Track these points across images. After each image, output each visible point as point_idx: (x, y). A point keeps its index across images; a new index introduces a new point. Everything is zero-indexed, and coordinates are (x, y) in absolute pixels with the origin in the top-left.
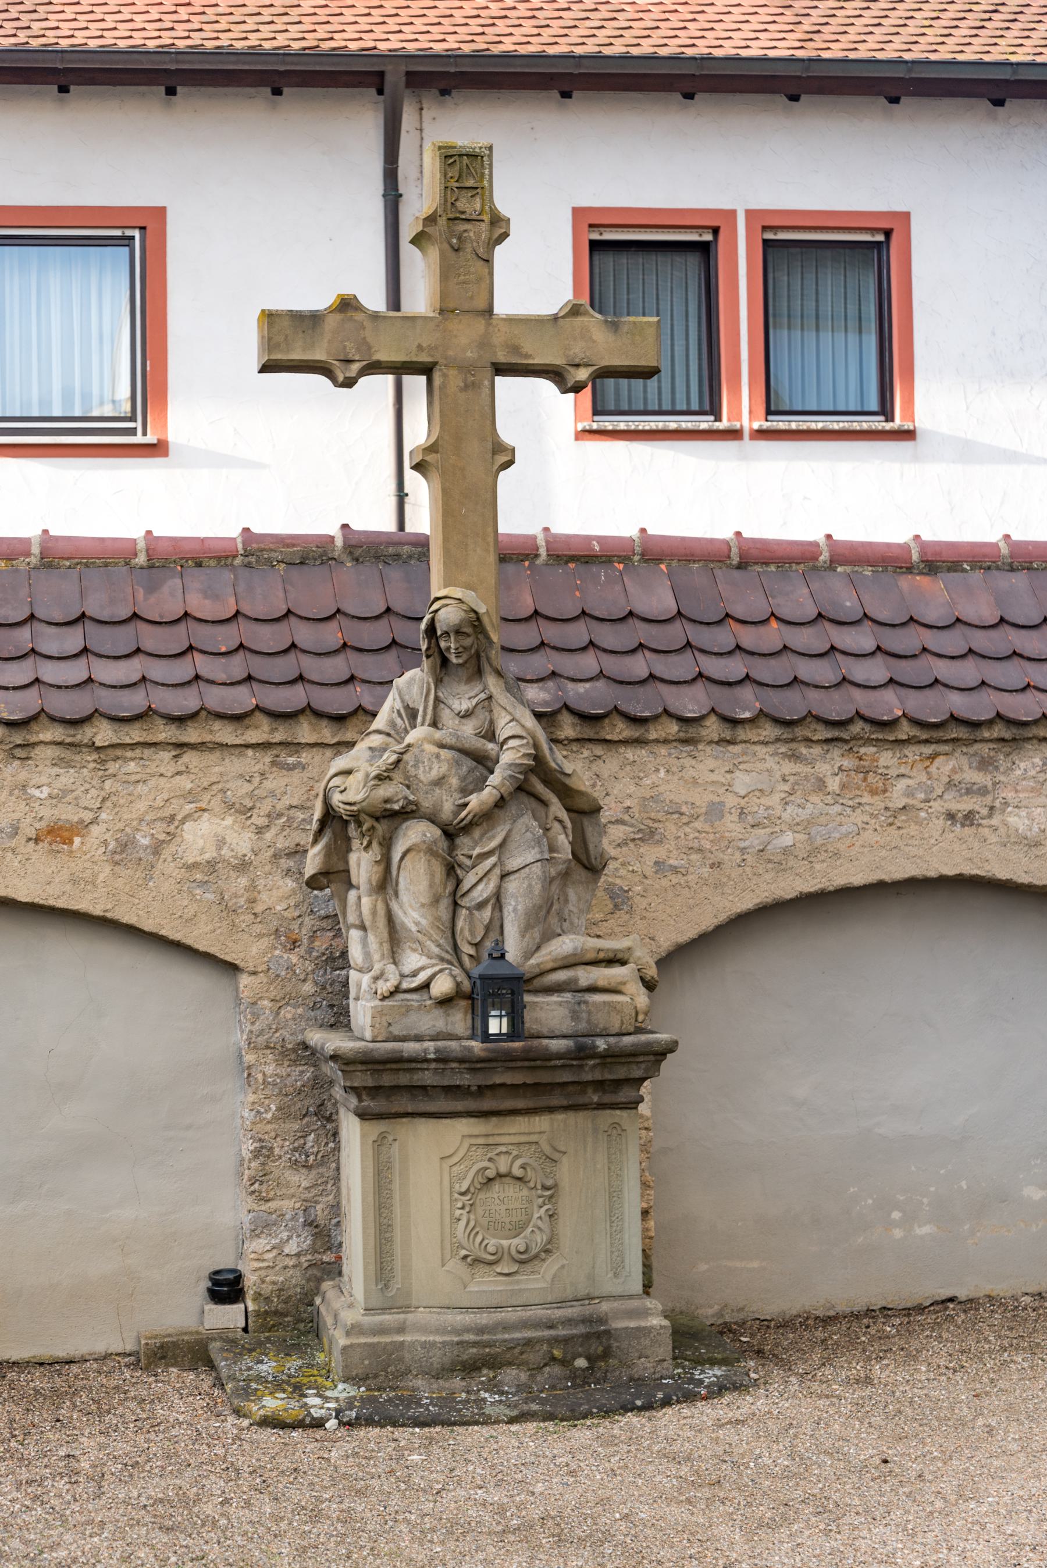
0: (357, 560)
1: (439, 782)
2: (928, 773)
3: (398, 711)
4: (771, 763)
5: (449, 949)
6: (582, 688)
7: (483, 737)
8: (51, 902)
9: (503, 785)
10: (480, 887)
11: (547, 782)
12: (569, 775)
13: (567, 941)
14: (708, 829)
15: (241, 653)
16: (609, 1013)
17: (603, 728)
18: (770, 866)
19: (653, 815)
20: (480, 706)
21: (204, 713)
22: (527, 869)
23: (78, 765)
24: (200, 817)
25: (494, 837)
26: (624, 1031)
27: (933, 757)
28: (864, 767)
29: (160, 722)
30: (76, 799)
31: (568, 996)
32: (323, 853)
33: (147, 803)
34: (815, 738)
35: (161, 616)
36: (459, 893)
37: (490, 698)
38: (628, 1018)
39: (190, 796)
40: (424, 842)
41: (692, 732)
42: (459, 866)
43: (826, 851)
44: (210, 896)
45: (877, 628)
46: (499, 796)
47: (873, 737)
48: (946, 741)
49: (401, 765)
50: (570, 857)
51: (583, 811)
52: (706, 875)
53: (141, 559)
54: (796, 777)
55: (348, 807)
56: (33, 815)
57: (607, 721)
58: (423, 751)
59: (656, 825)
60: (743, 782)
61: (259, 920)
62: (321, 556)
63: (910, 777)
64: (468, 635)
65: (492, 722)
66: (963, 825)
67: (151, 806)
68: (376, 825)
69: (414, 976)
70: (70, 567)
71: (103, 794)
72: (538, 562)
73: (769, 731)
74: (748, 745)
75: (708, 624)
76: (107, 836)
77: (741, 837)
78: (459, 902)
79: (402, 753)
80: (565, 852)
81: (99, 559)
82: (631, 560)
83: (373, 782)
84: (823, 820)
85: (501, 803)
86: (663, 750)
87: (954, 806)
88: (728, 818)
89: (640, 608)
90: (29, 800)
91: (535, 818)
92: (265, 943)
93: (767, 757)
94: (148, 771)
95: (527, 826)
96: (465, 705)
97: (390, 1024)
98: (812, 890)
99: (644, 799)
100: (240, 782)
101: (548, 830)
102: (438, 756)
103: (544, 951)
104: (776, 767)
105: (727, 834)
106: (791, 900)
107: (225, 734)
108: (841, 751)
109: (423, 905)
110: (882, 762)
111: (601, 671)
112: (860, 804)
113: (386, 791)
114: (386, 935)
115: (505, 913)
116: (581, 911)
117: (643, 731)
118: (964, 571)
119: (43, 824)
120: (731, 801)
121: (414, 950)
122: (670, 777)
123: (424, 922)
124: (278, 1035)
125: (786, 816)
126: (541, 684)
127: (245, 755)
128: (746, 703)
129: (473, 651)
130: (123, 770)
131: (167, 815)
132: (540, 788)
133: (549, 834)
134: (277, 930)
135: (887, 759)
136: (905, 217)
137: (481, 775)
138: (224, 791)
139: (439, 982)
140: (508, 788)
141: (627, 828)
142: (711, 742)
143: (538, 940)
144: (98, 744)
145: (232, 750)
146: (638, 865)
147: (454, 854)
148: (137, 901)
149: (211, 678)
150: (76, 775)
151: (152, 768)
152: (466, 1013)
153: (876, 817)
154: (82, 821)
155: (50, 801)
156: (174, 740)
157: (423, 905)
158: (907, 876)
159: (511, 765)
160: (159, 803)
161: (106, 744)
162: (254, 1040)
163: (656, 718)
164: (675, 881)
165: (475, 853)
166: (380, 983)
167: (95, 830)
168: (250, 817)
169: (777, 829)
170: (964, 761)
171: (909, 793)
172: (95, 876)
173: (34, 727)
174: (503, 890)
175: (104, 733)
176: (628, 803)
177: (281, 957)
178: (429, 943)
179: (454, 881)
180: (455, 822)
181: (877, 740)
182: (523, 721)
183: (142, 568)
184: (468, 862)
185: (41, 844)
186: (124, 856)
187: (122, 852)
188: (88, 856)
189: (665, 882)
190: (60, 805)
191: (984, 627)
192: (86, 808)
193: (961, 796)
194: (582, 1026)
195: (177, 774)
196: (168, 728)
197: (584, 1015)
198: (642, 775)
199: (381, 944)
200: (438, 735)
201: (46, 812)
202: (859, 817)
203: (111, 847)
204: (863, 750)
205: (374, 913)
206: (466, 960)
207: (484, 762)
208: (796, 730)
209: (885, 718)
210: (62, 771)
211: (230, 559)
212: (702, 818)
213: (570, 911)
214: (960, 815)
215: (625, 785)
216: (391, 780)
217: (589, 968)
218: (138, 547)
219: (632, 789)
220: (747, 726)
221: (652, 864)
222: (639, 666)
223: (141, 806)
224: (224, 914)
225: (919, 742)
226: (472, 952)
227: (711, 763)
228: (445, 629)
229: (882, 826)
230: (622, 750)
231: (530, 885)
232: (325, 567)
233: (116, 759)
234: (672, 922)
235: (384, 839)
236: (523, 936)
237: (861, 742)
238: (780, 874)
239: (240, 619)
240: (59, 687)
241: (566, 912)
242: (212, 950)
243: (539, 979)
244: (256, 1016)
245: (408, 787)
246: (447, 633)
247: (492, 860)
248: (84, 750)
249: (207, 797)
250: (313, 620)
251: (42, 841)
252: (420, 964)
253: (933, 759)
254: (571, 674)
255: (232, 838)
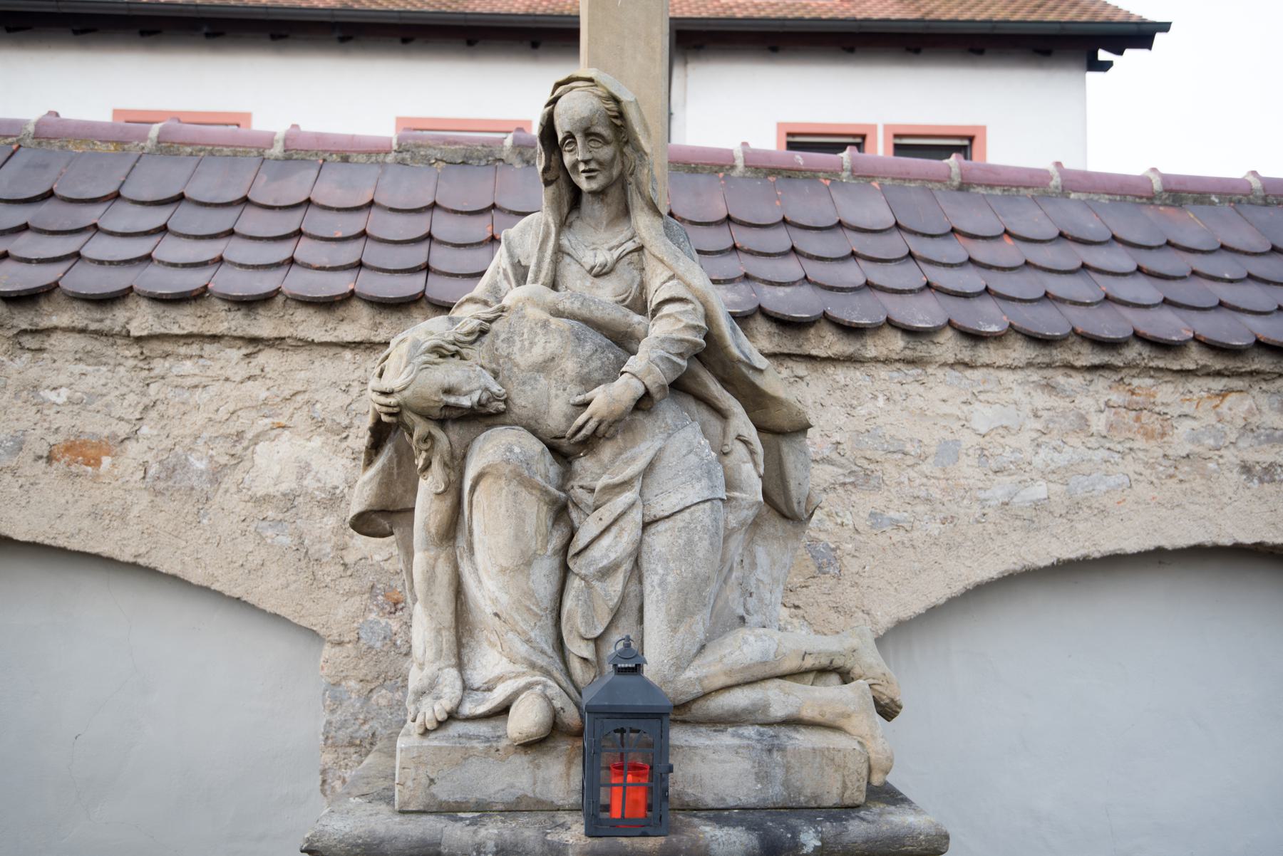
0: (528, 162)
1: (545, 366)
2: (1218, 414)
3: (505, 270)
4: (1018, 393)
5: (549, 651)
6: (781, 292)
7: (627, 306)
8: (61, 542)
9: (650, 372)
10: (606, 541)
11: (726, 382)
12: (761, 371)
13: (752, 639)
14: (938, 474)
15: (362, 241)
16: (821, 768)
17: (808, 340)
18: (1018, 523)
19: (868, 454)
20: (626, 260)
21: (280, 299)
22: (686, 514)
23: (112, 362)
24: (276, 436)
25: (633, 459)
26: (848, 802)
27: (1223, 394)
28: (1137, 403)
29: (221, 306)
30: (107, 406)
31: (750, 731)
32: (377, 479)
33: (205, 415)
34: (1078, 364)
35: (275, 201)
36: (572, 551)
37: (640, 249)
38: (854, 777)
39: (263, 407)
40: (508, 462)
41: (922, 349)
42: (576, 505)
43: (1090, 507)
44: (286, 540)
45: (1130, 250)
46: (641, 391)
47: (1151, 364)
48: (1240, 375)
49: (487, 339)
50: (761, 498)
51: (778, 428)
52: (936, 532)
53: (277, 150)
54: (1051, 413)
55: (383, 400)
56: (46, 425)
57: (812, 331)
58: (524, 317)
59: (872, 466)
60: (984, 416)
61: (349, 573)
62: (487, 156)
63: (1194, 418)
64: (606, 143)
65: (642, 287)
66: (1261, 481)
67: (210, 420)
68: (437, 432)
69: (489, 690)
70: (191, 154)
71: (146, 401)
72: (735, 174)
73: (1019, 352)
74: (991, 370)
75: (932, 236)
76: (149, 457)
77: (981, 485)
78: (571, 565)
79: (490, 321)
80: (753, 490)
81: (227, 146)
82: (838, 176)
83: (424, 358)
84: (1085, 467)
85: (644, 403)
86: (883, 372)
87: (1251, 457)
88: (964, 461)
89: (849, 218)
90: (40, 407)
91: (705, 433)
92: (356, 603)
93: (1014, 386)
94: (209, 373)
95: (690, 444)
96: (604, 257)
97: (432, 780)
98: (1073, 556)
99: (859, 433)
100: (333, 392)
101: (725, 454)
102: (545, 325)
103: (710, 656)
104: (1025, 399)
105: (962, 481)
106: (1046, 567)
107: (312, 326)
108: (1108, 383)
109: (503, 570)
110: (1159, 398)
111: (806, 277)
112: (1131, 449)
113: (449, 373)
114: (448, 617)
115: (647, 588)
116: (775, 581)
117: (858, 346)
118: (1212, 203)
119: (60, 438)
120: (968, 440)
121: (493, 645)
122: (891, 407)
123: (504, 599)
124: (366, 727)
125: (1038, 461)
126: (729, 286)
127: (343, 359)
128: (990, 318)
129: (615, 172)
130: (175, 371)
131: (233, 431)
132: (716, 389)
133: (727, 460)
134: (372, 587)
135: (1167, 393)
136: (983, 129)
137: (616, 357)
138: (311, 403)
139: (521, 709)
140: (658, 378)
141: (836, 469)
142: (944, 364)
143: (701, 636)
144: (134, 333)
145: (324, 350)
146: (849, 516)
147: (569, 486)
148: (184, 543)
149: (307, 261)
150: (110, 375)
151: (215, 370)
152: (570, 763)
153: (1152, 466)
154: (115, 436)
155: (70, 408)
156: (239, 333)
157: (503, 570)
158: (1192, 542)
159: (663, 341)
160: (223, 415)
161: (145, 333)
162: (333, 734)
163: (875, 329)
164: (896, 538)
165: (599, 485)
166: (427, 701)
167: (132, 447)
168: (346, 438)
169: (1026, 476)
170: (1263, 401)
171: (1195, 438)
172: (125, 509)
173: (46, 306)
174: (645, 548)
175: (142, 319)
176: (837, 437)
177: (378, 623)
178: (510, 635)
179: (566, 531)
180: (570, 431)
181: (1158, 369)
182: (688, 278)
183: (277, 159)
184: (589, 499)
185: (55, 464)
186: (170, 483)
187: (168, 478)
188: (120, 482)
189: (882, 540)
190: (84, 413)
191: (1255, 254)
192: (120, 419)
193: (1260, 444)
194: (775, 792)
195: (249, 378)
196: (231, 315)
197: (779, 773)
198: (855, 402)
199: (439, 632)
200: (551, 296)
201: (63, 421)
202: (1130, 466)
203: (152, 472)
204: (1136, 382)
205: (430, 578)
206: (576, 666)
207: (623, 341)
208: (1054, 352)
209: (1175, 338)
210: (90, 369)
211: (382, 156)
212: (930, 460)
213: (758, 580)
214: (1258, 468)
215: (834, 414)
216: (462, 358)
217: (787, 684)
218: (276, 137)
219: (842, 420)
220: (991, 346)
221: (866, 516)
222: (852, 274)
223: (199, 418)
224: (303, 563)
225: (1208, 375)
226: (587, 651)
227: (943, 391)
228: (567, 128)
229: (1159, 478)
230: (830, 370)
231: (690, 542)
232: (491, 169)
233: (166, 356)
234: (892, 592)
235: (453, 457)
236: (675, 630)
237: (1134, 372)
238: (1031, 534)
239: (373, 210)
240: (101, 262)
241: (753, 582)
242: (282, 612)
243: (701, 702)
244: (337, 701)
245: (496, 375)
246: (570, 136)
247: (628, 496)
248: (119, 342)
249: (288, 409)
250: (462, 213)
251: (58, 460)
252: (497, 671)
253: (1224, 396)
254: (769, 277)
255: (318, 464)
